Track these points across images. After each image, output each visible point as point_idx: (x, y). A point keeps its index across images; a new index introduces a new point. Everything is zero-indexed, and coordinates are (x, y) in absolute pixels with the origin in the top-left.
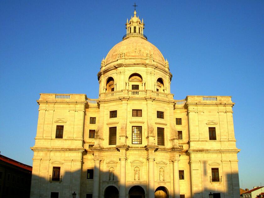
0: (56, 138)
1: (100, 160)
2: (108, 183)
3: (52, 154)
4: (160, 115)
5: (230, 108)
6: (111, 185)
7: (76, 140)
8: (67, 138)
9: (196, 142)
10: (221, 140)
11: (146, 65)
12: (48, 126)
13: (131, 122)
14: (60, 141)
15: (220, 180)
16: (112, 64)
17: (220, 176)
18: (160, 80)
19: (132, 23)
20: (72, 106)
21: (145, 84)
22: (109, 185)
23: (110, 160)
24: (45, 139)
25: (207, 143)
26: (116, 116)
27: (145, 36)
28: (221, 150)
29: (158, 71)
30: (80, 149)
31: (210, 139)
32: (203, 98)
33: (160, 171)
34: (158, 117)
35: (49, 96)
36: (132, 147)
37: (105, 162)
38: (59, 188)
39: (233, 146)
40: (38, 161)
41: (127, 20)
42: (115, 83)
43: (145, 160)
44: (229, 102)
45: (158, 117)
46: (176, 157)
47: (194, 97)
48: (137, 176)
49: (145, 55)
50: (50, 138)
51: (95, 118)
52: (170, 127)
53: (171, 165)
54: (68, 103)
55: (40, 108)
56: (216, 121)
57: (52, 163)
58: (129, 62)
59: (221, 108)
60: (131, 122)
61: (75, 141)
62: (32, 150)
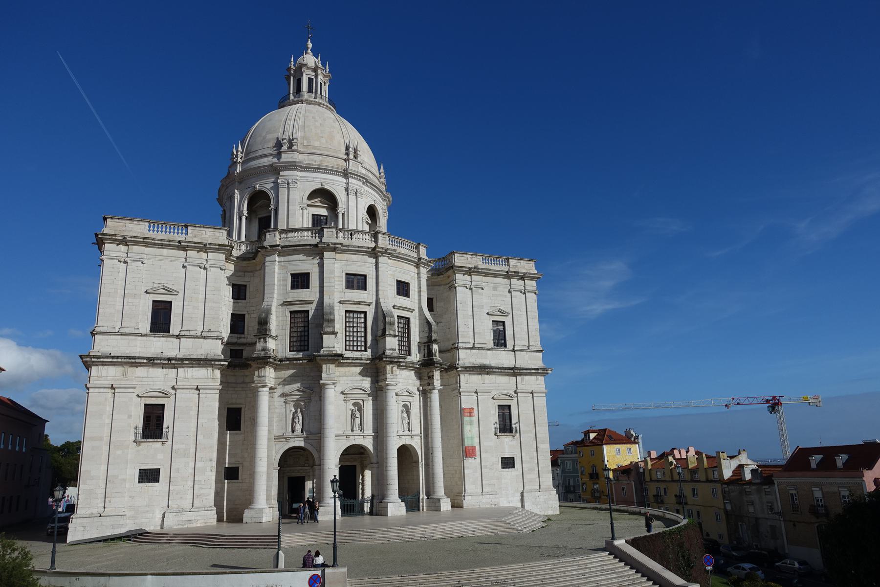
0: (151, 331)
1: (270, 385)
2: (287, 439)
3: (141, 372)
4: (403, 289)
5: (531, 284)
7: (205, 338)
8: (182, 333)
9: (468, 351)
10: (516, 348)
11: (346, 174)
12: (130, 300)
14: (162, 339)
15: (514, 430)
17: (514, 420)
18: (372, 212)
20: (192, 253)
21: (343, 214)
22: (291, 444)
24: (122, 334)
25: (489, 352)
26: (306, 285)
27: (330, 101)
28: (518, 369)
29: (370, 190)
31: (495, 344)
33: (403, 412)
36: (348, 359)
38: (160, 456)
39: (535, 360)
40: (102, 390)
42: (272, 206)
45: (398, 294)
48: (358, 421)
50: (136, 331)
51: (245, 286)
52: (420, 315)
54: (181, 246)
58: (308, 162)
59: (517, 283)
60: (340, 302)
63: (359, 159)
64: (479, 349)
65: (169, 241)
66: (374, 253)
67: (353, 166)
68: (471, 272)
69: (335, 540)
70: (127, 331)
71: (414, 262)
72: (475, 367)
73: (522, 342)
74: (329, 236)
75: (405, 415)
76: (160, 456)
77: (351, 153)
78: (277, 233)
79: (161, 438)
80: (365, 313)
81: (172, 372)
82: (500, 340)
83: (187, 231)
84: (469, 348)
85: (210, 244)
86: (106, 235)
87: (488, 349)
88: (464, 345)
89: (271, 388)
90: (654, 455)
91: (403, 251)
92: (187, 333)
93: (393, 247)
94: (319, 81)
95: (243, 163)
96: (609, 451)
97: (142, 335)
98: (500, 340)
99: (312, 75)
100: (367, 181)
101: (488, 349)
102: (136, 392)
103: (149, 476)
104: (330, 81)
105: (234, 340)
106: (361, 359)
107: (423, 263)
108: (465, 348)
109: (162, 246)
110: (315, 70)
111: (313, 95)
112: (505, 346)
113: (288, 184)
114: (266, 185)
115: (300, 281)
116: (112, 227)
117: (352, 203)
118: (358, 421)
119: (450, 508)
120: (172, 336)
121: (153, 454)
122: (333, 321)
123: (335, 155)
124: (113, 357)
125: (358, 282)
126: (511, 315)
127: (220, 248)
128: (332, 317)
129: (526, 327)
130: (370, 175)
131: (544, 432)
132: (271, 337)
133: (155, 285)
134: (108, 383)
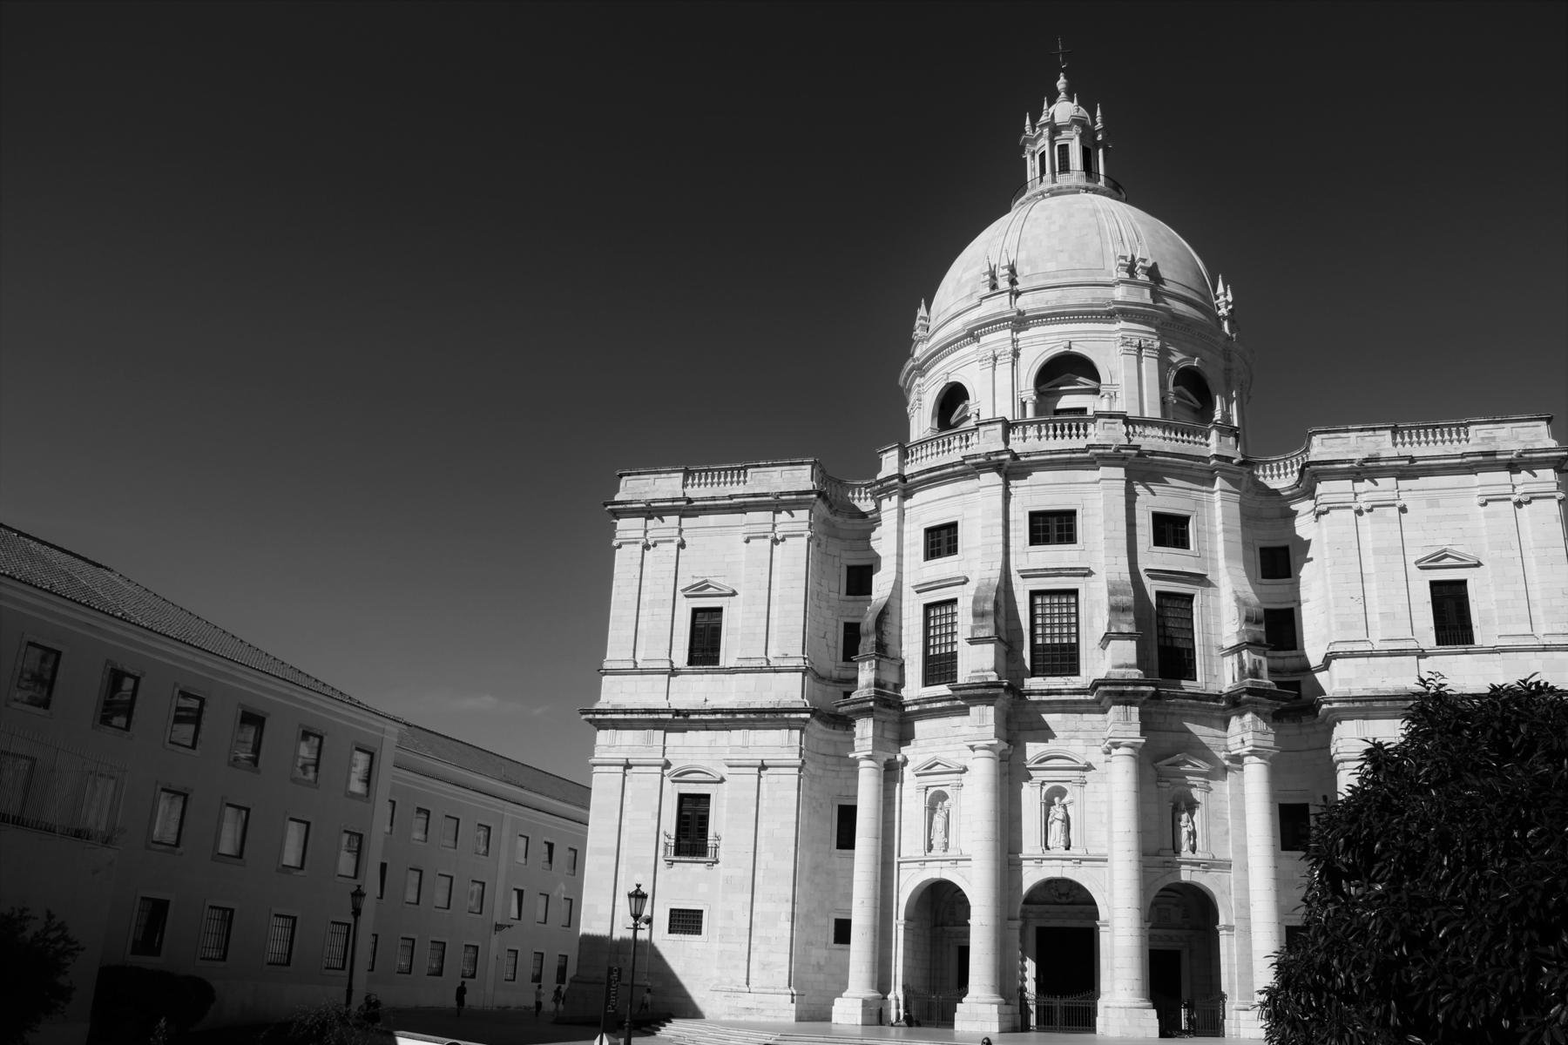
0: (690, 663)
12: (656, 610)
13: (1025, 575)
16: (957, 326)
23: (930, 756)
24: (643, 672)
26: (953, 550)
31: (1441, 640)
32: (1394, 438)
38: (703, 888)
40: (613, 769)
43: (1095, 756)
44: (1538, 446)
47: (1347, 431)
48: (1056, 828)
55: (618, 535)
57: (680, 776)
62: (590, 721)
65: (714, 498)
76: (703, 888)
79: (704, 854)
80: (1075, 592)
87: (1422, 654)
92: (746, 664)
97: (673, 672)
105: (849, 674)
106: (1059, 692)
109: (706, 510)
112: (1469, 639)
113: (995, 359)
115: (942, 540)
118: (1056, 828)
123: (1090, 279)
124: (625, 712)
125: (1060, 528)
134: (621, 756)
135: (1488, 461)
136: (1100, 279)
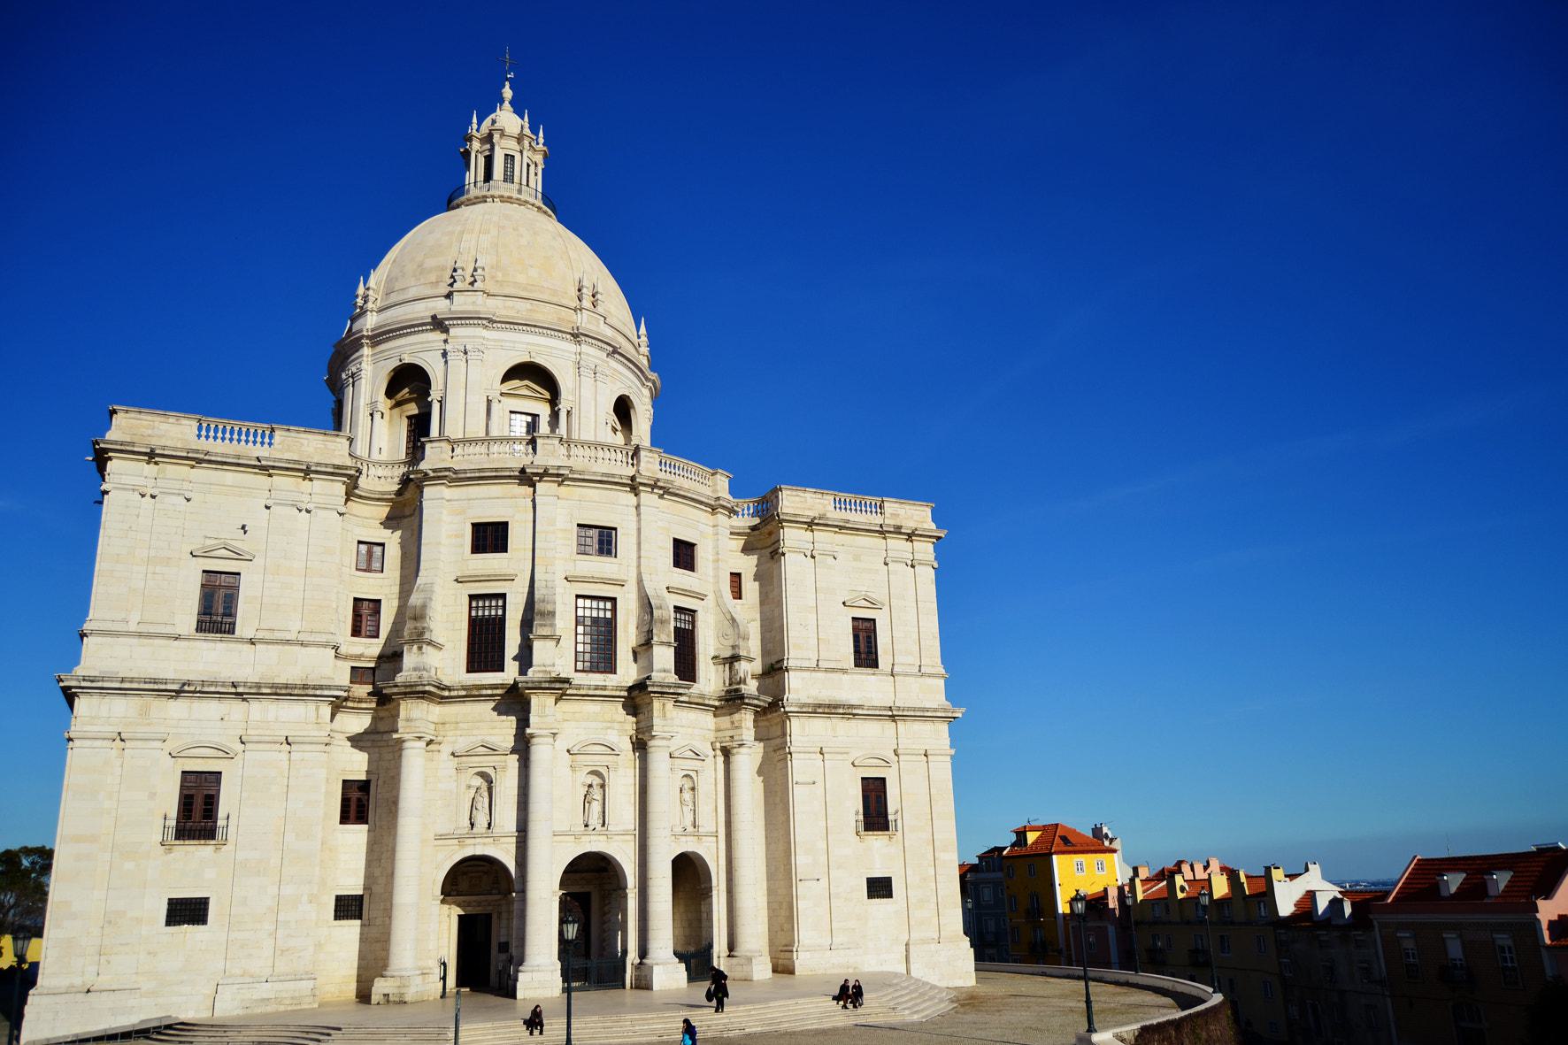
1: (428, 738)
2: (460, 839)
4: (684, 554)
5: (925, 550)
6: (479, 851)
8: (260, 635)
14: (220, 646)
16: (423, 311)
17: (891, 810)
18: (623, 408)
19: (496, 137)
20: (282, 482)
22: (468, 852)
24: (140, 635)
27: (548, 199)
28: (899, 709)
30: (329, 687)
34: (677, 564)
35: (164, 427)
36: (579, 687)
37: (446, 749)
40: (98, 743)
41: (475, 120)
45: (677, 564)
46: (744, 731)
49: (574, 293)
50: (168, 630)
53: (721, 759)
54: (265, 469)
56: (879, 595)
58: (504, 312)
59: (898, 545)
61: (297, 648)
63: (600, 309)
64: (827, 670)
65: (238, 457)
66: (634, 486)
67: (585, 321)
68: (811, 525)
69: (569, 1034)
70: (152, 629)
71: (707, 505)
72: (820, 706)
73: (906, 661)
74: (550, 455)
75: (687, 795)
77: (585, 296)
78: (446, 447)
80: (613, 600)
81: (235, 708)
82: (866, 651)
83: (271, 437)
84: (808, 669)
85: (318, 464)
86: (115, 442)
87: (844, 671)
88: (799, 664)
89: (429, 743)
90: (1144, 873)
91: (686, 484)
92: (268, 635)
93: (668, 476)
94: (526, 160)
95: (380, 311)
96: (1062, 866)
98: (866, 651)
99: (513, 144)
100: (615, 351)
101: (844, 671)
102: (168, 747)
103: (187, 911)
104: (545, 158)
106: (604, 688)
107: (723, 507)
108: (801, 669)
110: (520, 139)
111: (516, 186)
114: (421, 350)
115: (490, 537)
116: (127, 426)
117: (587, 393)
118: (596, 807)
119: (769, 974)
120: (241, 640)
121: (194, 867)
122: (552, 614)
126: (886, 608)
127: (335, 472)
128: (549, 608)
129: (912, 629)
130: (621, 339)
131: (947, 829)
132: (430, 643)
133: (209, 542)
134: (111, 730)
135: (898, 530)
136: (564, 302)
